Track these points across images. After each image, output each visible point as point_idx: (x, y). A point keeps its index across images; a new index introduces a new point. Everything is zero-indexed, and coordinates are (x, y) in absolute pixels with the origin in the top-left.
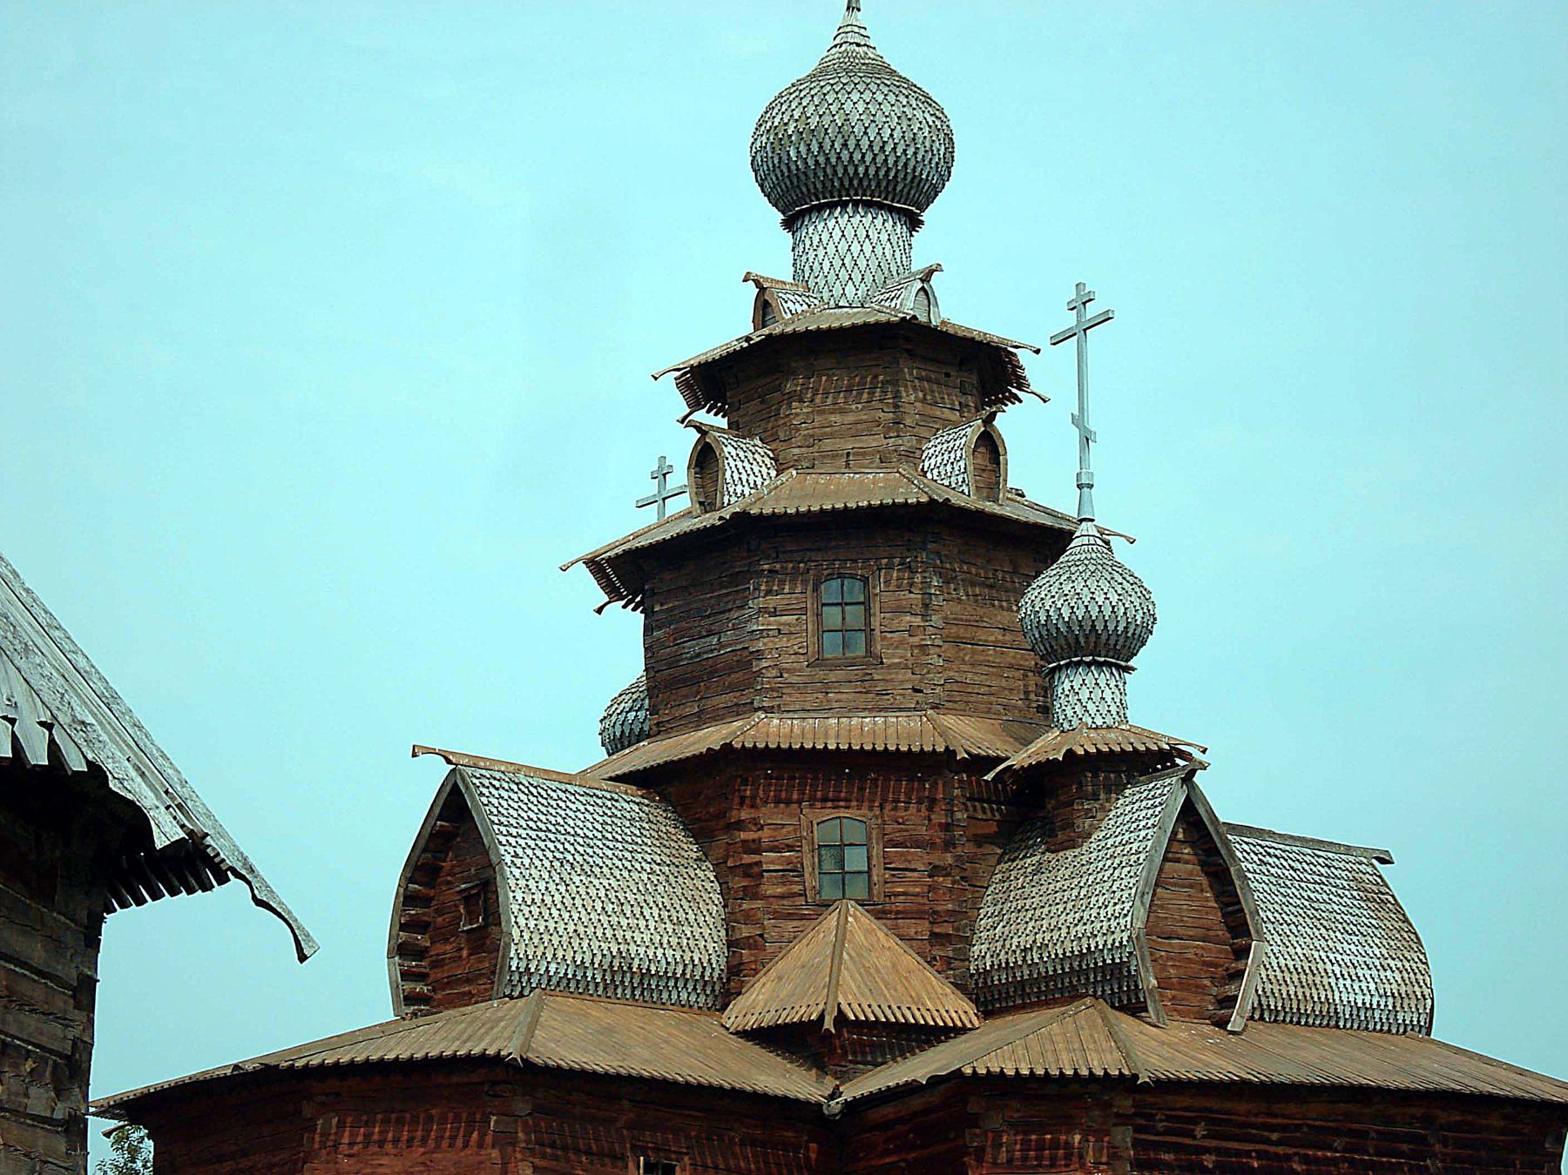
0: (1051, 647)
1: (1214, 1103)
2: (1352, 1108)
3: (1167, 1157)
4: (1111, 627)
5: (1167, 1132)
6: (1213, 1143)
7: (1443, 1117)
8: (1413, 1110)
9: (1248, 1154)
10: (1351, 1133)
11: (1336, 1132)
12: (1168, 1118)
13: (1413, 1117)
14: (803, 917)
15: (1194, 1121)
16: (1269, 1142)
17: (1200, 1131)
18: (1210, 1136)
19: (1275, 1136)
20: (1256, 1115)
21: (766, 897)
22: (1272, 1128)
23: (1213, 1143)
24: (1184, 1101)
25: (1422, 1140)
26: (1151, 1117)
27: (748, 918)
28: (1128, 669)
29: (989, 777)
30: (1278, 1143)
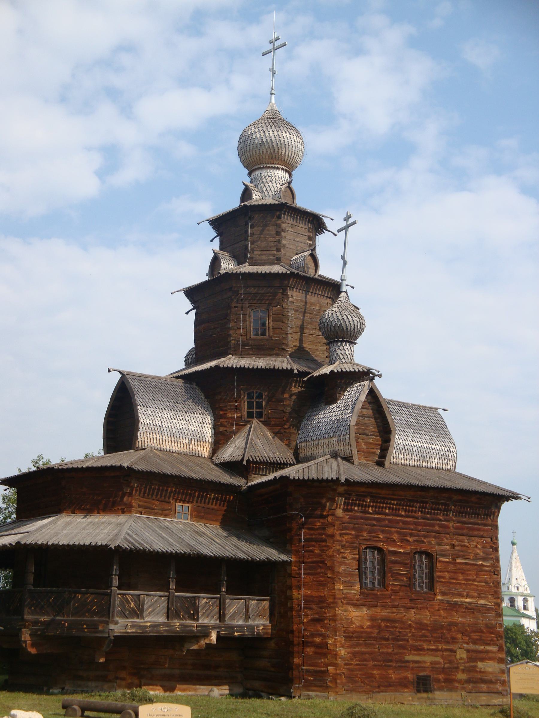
0: (329, 335)
1: (374, 491)
2: (423, 493)
4: (349, 329)
7: (455, 497)
8: (444, 495)
11: (417, 502)
12: (357, 495)
14: (242, 425)
15: (366, 496)
21: (229, 418)
22: (394, 500)
24: (363, 489)
27: (222, 425)
28: (355, 343)
29: (305, 379)
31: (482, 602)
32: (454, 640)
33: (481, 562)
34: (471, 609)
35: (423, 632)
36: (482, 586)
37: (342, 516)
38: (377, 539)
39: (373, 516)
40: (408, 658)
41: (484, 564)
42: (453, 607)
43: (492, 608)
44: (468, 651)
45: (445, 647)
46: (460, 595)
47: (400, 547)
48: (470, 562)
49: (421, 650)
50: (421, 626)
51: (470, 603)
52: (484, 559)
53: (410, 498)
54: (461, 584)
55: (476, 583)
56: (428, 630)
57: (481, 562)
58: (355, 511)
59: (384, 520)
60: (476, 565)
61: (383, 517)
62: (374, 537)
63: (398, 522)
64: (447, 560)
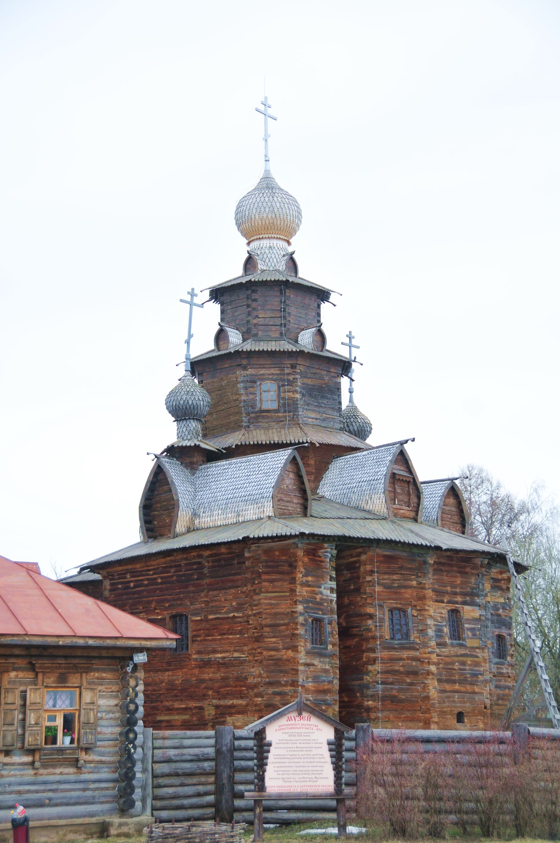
3: (120, 586)
5: (119, 579)
6: (133, 579)
7: (207, 553)
8: (193, 554)
9: (143, 580)
10: (175, 566)
11: (171, 567)
12: (118, 575)
13: (194, 556)
15: (126, 573)
16: (149, 575)
17: (128, 576)
18: (132, 577)
19: (151, 573)
20: (143, 567)
22: (149, 570)
23: (133, 579)
25: (200, 563)
26: (113, 575)
30: (152, 575)
31: (236, 655)
32: (204, 697)
33: (232, 614)
34: (224, 664)
35: (175, 692)
36: (236, 639)
37: (108, 596)
38: (138, 611)
39: (134, 590)
40: (159, 718)
41: (236, 615)
42: (205, 664)
43: (246, 660)
44: (217, 707)
45: (194, 705)
46: (215, 651)
47: (158, 614)
48: (221, 616)
49: (172, 710)
50: (171, 687)
51: (223, 658)
52: (237, 610)
53: (164, 565)
54: (215, 640)
55: (231, 636)
56: (178, 690)
57: (232, 614)
58: (119, 589)
59: (143, 591)
60: (229, 618)
61: (142, 589)
62: (135, 609)
63: (156, 590)
64: (199, 618)
